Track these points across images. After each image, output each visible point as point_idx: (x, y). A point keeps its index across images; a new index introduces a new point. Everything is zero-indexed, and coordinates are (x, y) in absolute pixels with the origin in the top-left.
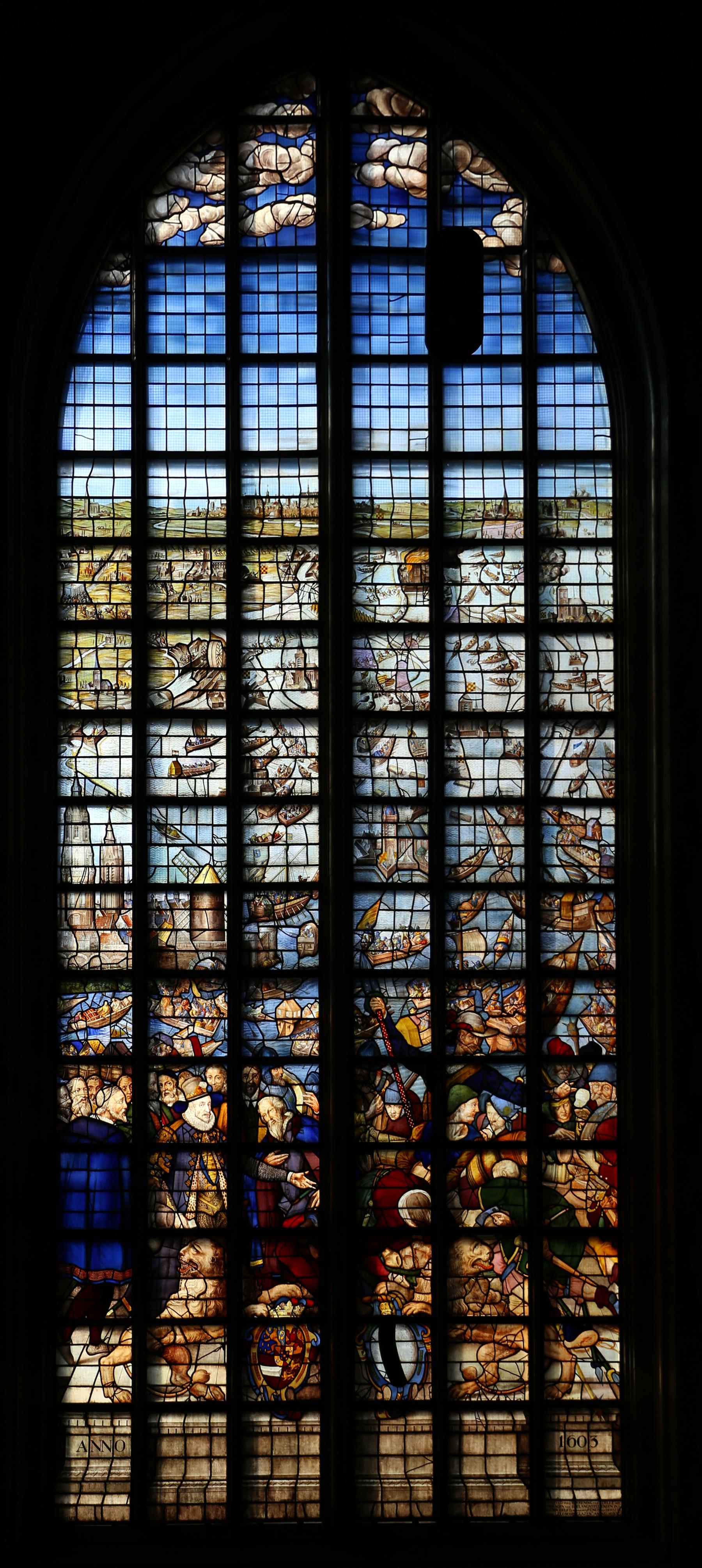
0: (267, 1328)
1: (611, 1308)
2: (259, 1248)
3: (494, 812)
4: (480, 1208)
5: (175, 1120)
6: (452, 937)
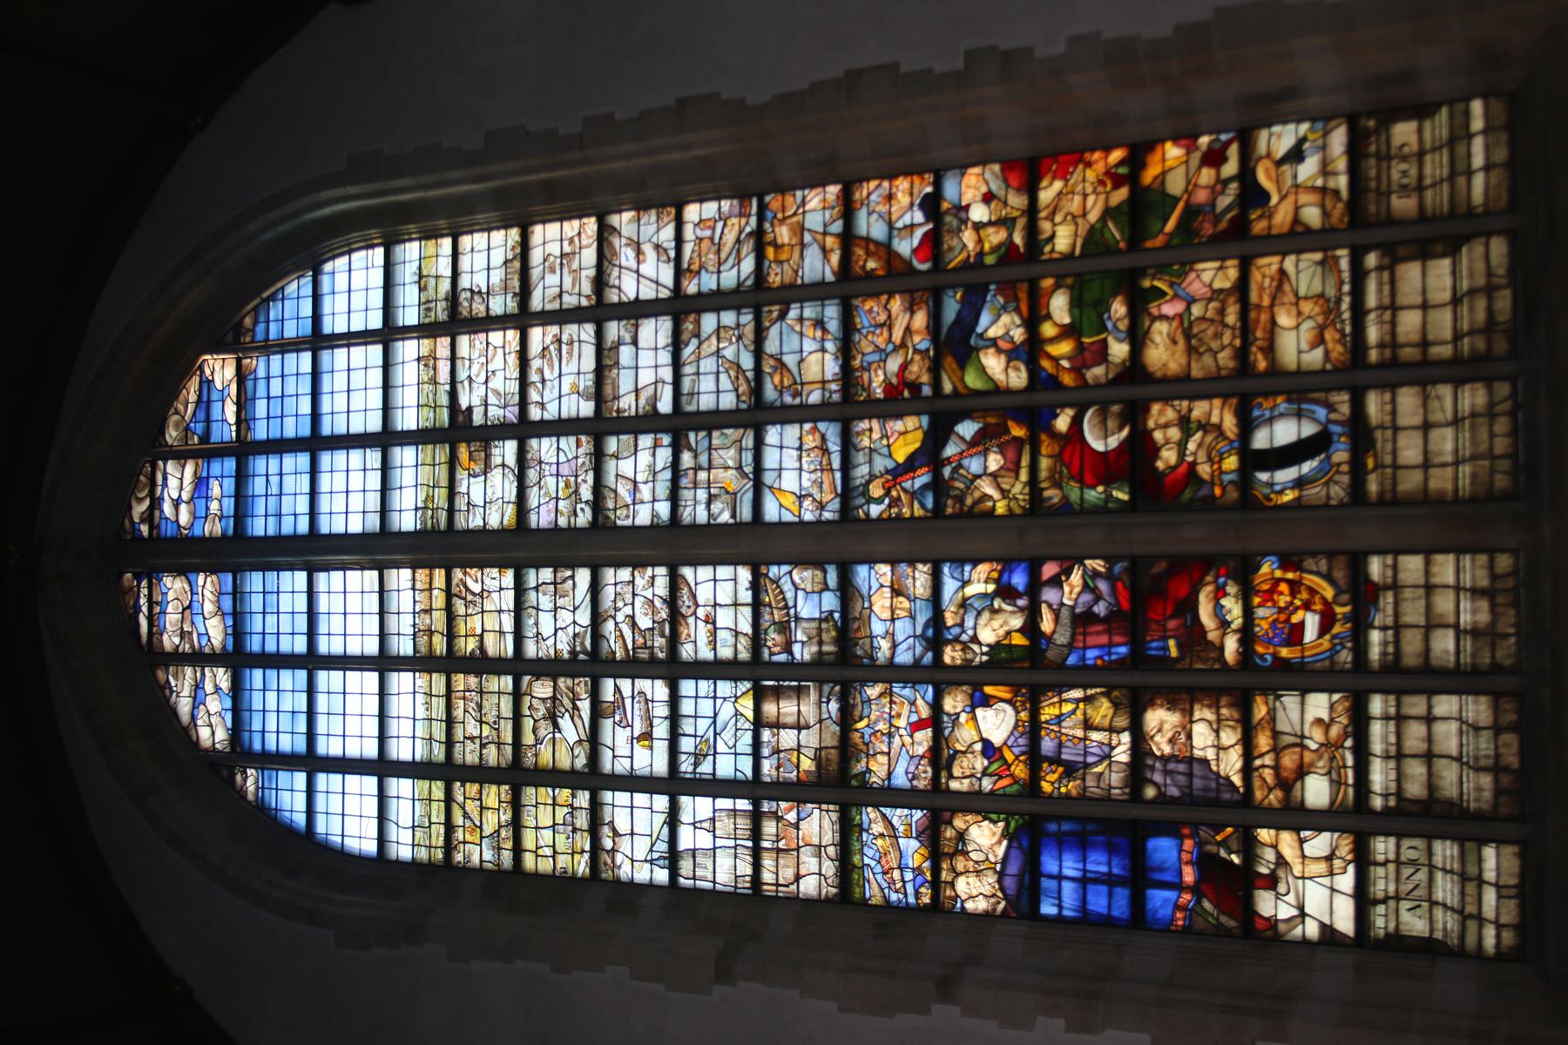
0: (1255, 635)
1: (1228, 144)
2: (1154, 644)
3: (687, 352)
4: (1105, 341)
5: (1002, 757)
6: (808, 395)
